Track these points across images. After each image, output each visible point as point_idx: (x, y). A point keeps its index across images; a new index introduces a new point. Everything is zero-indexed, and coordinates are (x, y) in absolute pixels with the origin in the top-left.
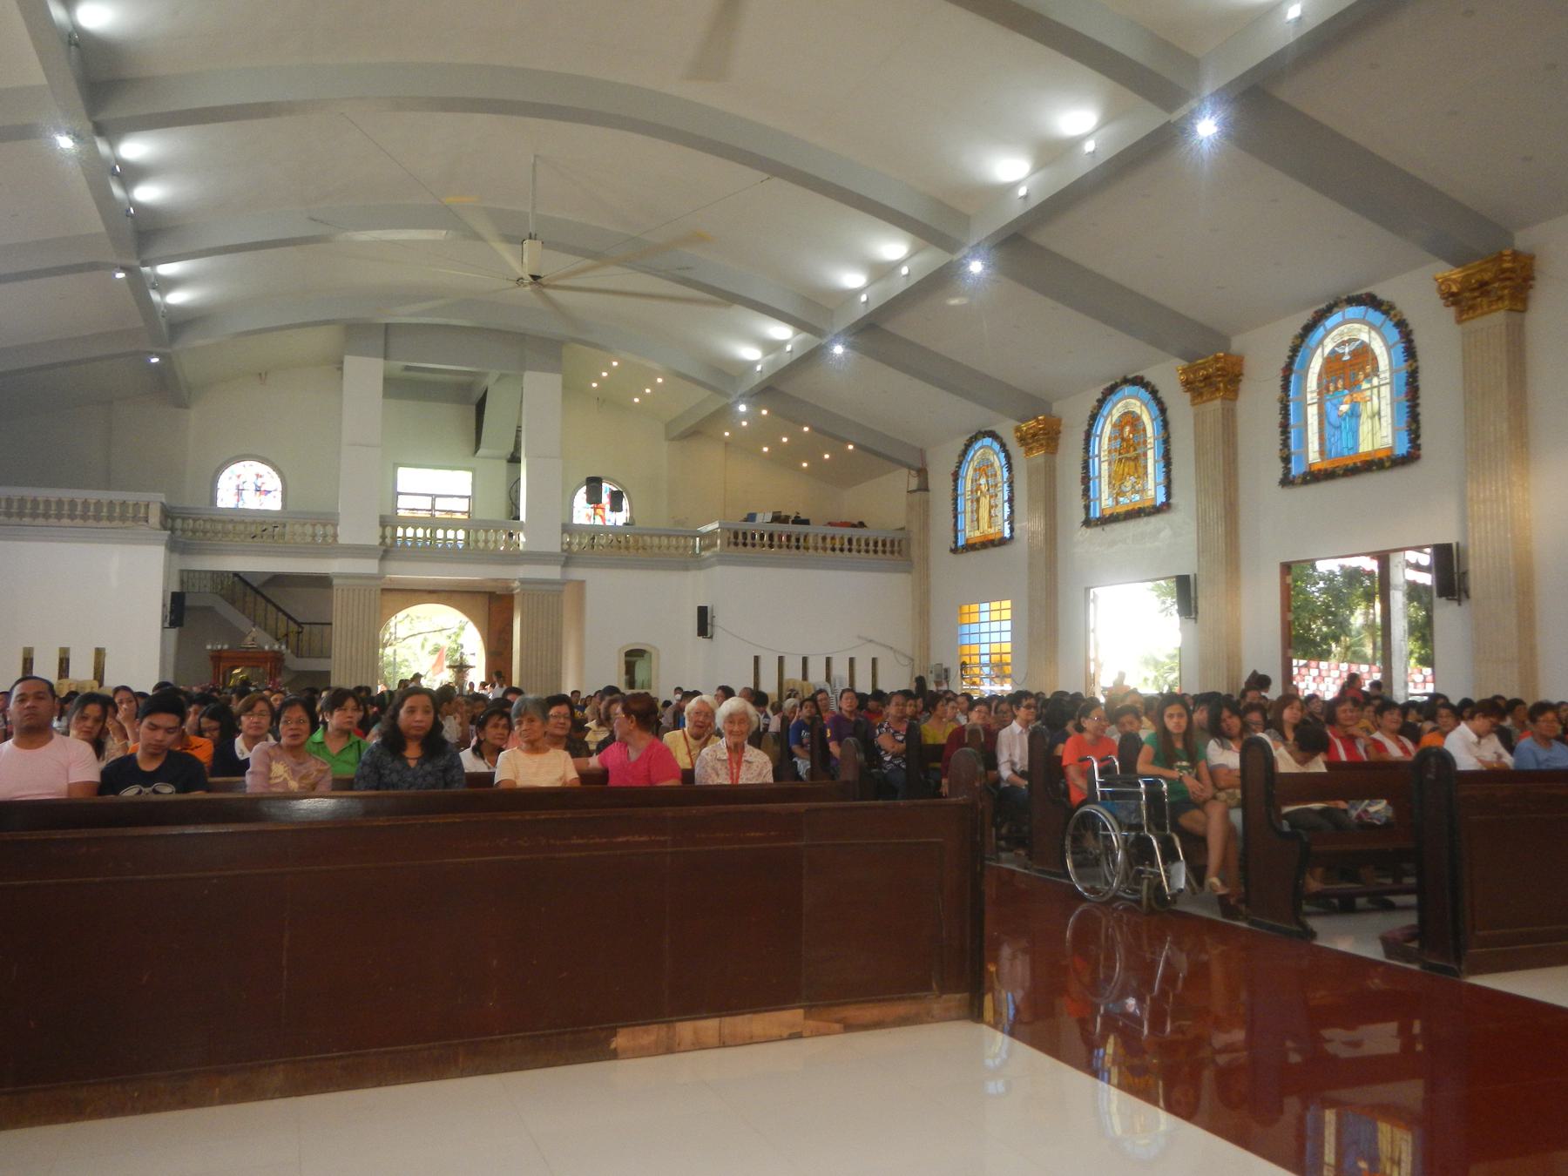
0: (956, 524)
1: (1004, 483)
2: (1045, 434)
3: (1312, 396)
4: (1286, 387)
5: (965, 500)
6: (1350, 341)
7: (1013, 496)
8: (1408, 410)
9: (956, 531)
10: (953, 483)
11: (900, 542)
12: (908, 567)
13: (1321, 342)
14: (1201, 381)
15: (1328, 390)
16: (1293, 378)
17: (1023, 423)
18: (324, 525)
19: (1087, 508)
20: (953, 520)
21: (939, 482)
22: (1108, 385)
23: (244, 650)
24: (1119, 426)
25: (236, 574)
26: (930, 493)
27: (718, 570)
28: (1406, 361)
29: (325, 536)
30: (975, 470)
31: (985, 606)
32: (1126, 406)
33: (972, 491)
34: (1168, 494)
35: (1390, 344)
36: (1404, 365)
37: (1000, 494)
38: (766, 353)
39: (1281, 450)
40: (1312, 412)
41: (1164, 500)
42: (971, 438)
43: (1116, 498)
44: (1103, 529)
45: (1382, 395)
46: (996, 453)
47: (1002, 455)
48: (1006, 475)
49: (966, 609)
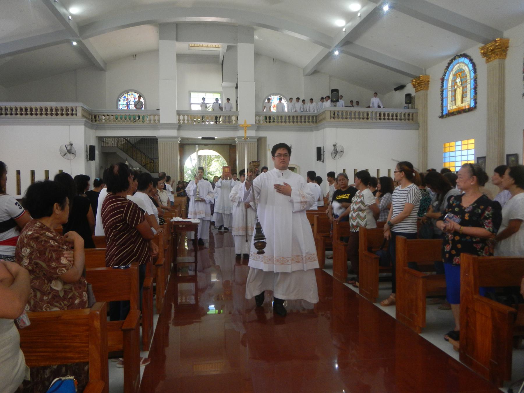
0: (442, 104)
1: (471, 79)
7: (477, 85)
9: (442, 107)
10: (441, 84)
11: (412, 114)
12: (417, 127)
18: (155, 116)
20: (441, 102)
25: (125, 138)
29: (155, 120)
30: (454, 75)
31: (459, 143)
33: (452, 86)
38: (348, 22)
46: (466, 64)
47: (470, 66)
48: (473, 75)
49: (447, 145)
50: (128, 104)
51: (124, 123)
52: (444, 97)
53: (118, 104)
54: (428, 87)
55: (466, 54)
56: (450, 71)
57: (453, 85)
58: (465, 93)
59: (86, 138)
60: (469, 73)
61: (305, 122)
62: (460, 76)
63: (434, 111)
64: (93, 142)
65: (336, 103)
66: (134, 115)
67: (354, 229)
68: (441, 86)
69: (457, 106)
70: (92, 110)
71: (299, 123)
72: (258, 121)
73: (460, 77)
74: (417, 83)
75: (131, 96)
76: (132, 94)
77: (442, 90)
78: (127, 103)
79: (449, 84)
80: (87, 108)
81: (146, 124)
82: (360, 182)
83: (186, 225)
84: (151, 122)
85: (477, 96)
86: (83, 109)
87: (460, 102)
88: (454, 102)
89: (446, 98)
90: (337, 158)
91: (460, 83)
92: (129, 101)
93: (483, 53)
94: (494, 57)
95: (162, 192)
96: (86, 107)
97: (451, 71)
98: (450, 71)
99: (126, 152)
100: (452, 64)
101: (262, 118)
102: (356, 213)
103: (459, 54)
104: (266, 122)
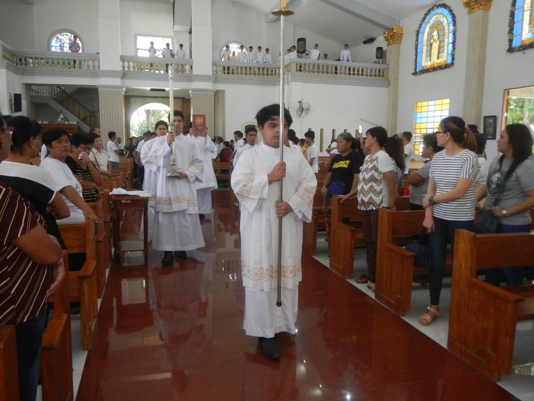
0: (416, 59)
1: (449, 33)
9: (416, 63)
10: (416, 37)
11: (383, 70)
12: (388, 85)
18: (94, 61)
19: (511, 41)
20: (415, 57)
23: (57, 124)
25: (58, 86)
29: (94, 67)
30: (430, 28)
31: (432, 103)
33: (427, 40)
37: (446, 40)
44: (523, 53)
46: (444, 16)
48: (452, 28)
49: (419, 104)
50: (62, 46)
51: (56, 68)
52: (419, 51)
53: (49, 46)
54: (401, 40)
55: (445, 4)
56: (427, 23)
57: (429, 38)
58: (442, 48)
60: (447, 26)
61: (267, 75)
62: (437, 29)
64: (19, 90)
65: (302, 54)
66: (69, 59)
67: (364, 207)
68: (416, 39)
69: (433, 62)
71: (261, 76)
73: (438, 30)
74: (389, 36)
75: (65, 36)
76: (67, 35)
77: (417, 44)
78: (60, 45)
79: (424, 38)
80: (9, 48)
81: (84, 70)
82: (375, 142)
83: (131, 200)
84: (90, 67)
85: (455, 51)
86: (3, 49)
88: (429, 58)
89: (421, 53)
90: (303, 116)
91: (436, 36)
92: (63, 43)
93: (466, 2)
94: (477, 8)
95: (100, 153)
96: (8, 47)
97: (428, 23)
98: (427, 23)
99: (61, 103)
100: (429, 15)
101: (220, 69)
102: (368, 185)
103: (437, 4)
104: (224, 73)
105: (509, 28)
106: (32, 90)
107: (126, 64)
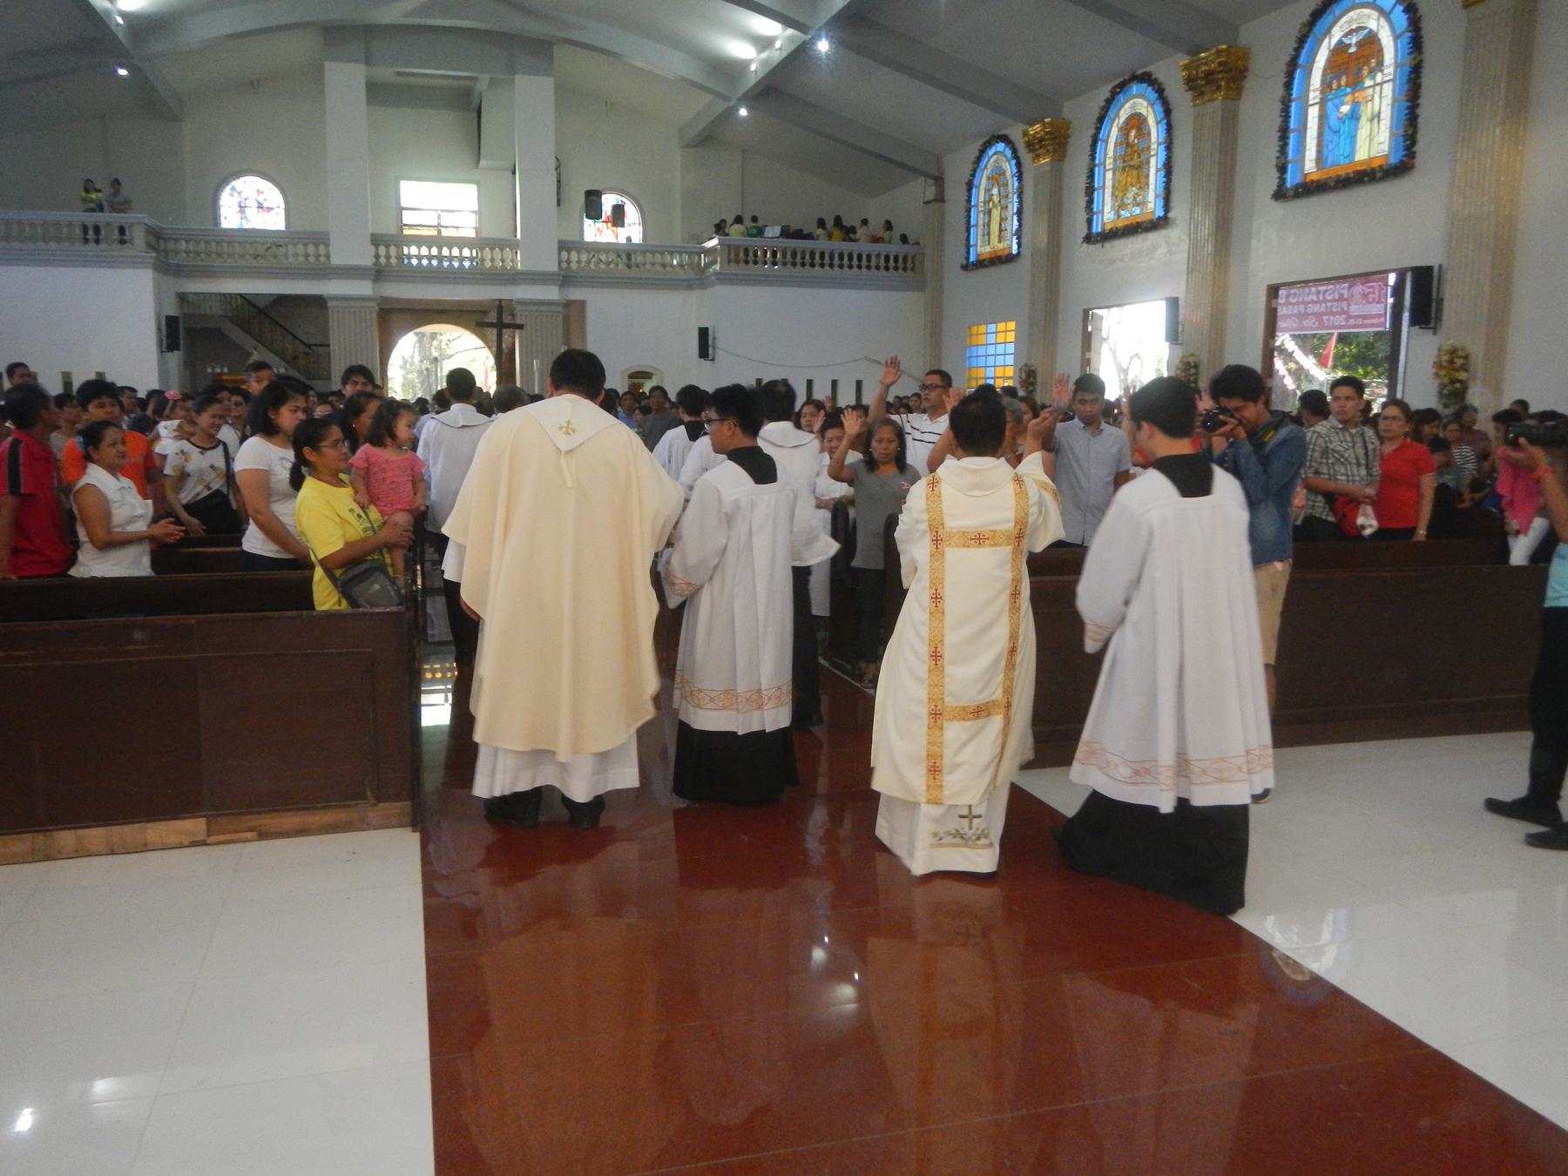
2: (1052, 139)
3: (1314, 96)
4: (1288, 86)
5: (979, 212)
6: (1360, 29)
8: (1406, 111)
9: (968, 246)
11: (913, 258)
12: (920, 286)
13: (1328, 32)
14: (1202, 78)
15: (1331, 89)
16: (1298, 74)
17: (1031, 126)
18: (316, 245)
20: (966, 234)
21: (954, 191)
22: (1117, 82)
24: (1125, 130)
25: (241, 295)
26: (946, 205)
27: (720, 290)
28: (1409, 54)
29: (318, 256)
30: (988, 179)
31: (992, 327)
32: (1133, 106)
33: (985, 203)
34: (1167, 206)
35: (1398, 32)
36: (1409, 58)
37: (1010, 206)
39: (1278, 158)
40: (1313, 112)
41: (1160, 213)
42: (985, 143)
43: (1118, 211)
44: (1103, 246)
45: (1383, 95)
47: (1013, 162)
48: (1016, 184)
57: (987, 199)
59: (158, 300)
63: (953, 258)
68: (967, 198)
70: (160, 227)
72: (566, 262)
80: (150, 223)
87: (996, 240)
88: (986, 237)
105: (1087, 198)
106: (188, 302)
107: (382, 250)
